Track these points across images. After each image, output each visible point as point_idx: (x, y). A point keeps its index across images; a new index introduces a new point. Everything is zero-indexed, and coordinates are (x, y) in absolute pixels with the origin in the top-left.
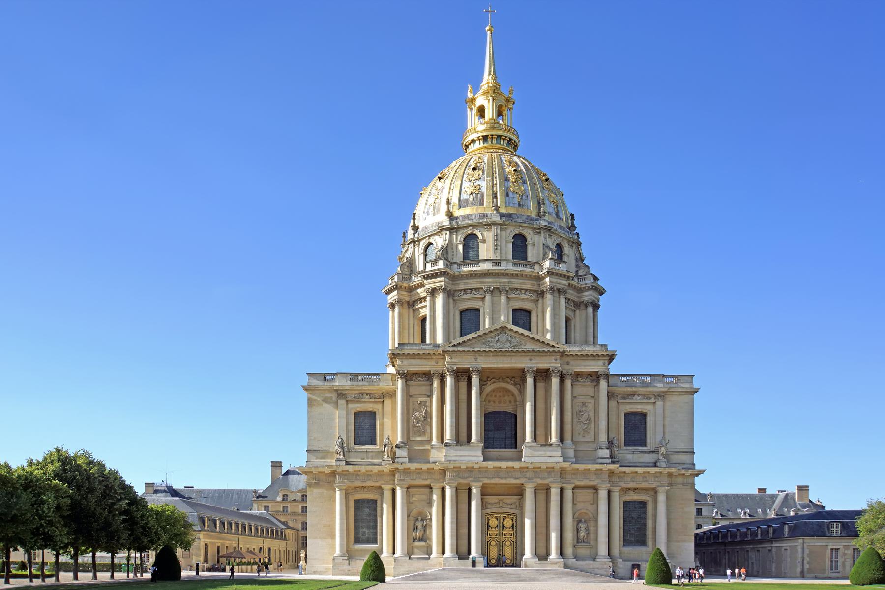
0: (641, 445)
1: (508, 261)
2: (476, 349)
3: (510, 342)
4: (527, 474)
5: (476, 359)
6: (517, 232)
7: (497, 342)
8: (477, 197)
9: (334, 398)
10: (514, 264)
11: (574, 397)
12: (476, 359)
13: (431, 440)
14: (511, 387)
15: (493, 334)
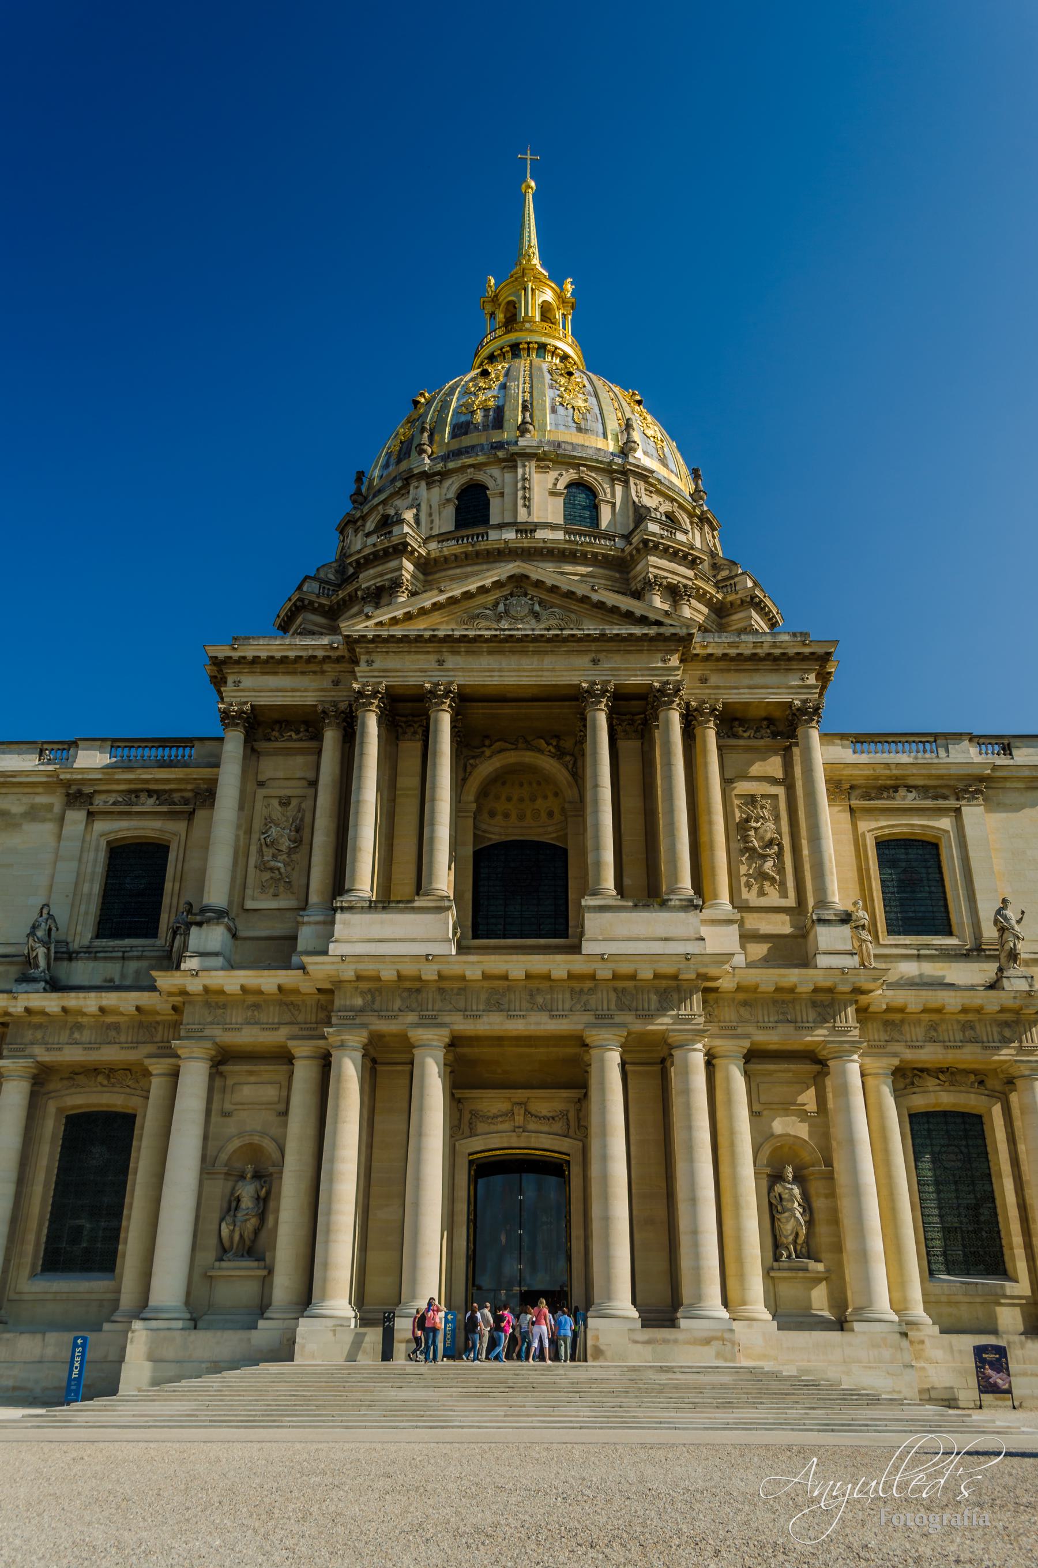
0: (936, 933)
1: (553, 527)
2: (441, 634)
3: (537, 616)
4: (593, 1001)
5: (441, 662)
6: (576, 476)
7: (499, 618)
8: (486, 416)
9: (57, 809)
10: (567, 532)
11: (727, 782)
12: (441, 662)
13: (304, 906)
14: (548, 764)
15: (491, 598)
